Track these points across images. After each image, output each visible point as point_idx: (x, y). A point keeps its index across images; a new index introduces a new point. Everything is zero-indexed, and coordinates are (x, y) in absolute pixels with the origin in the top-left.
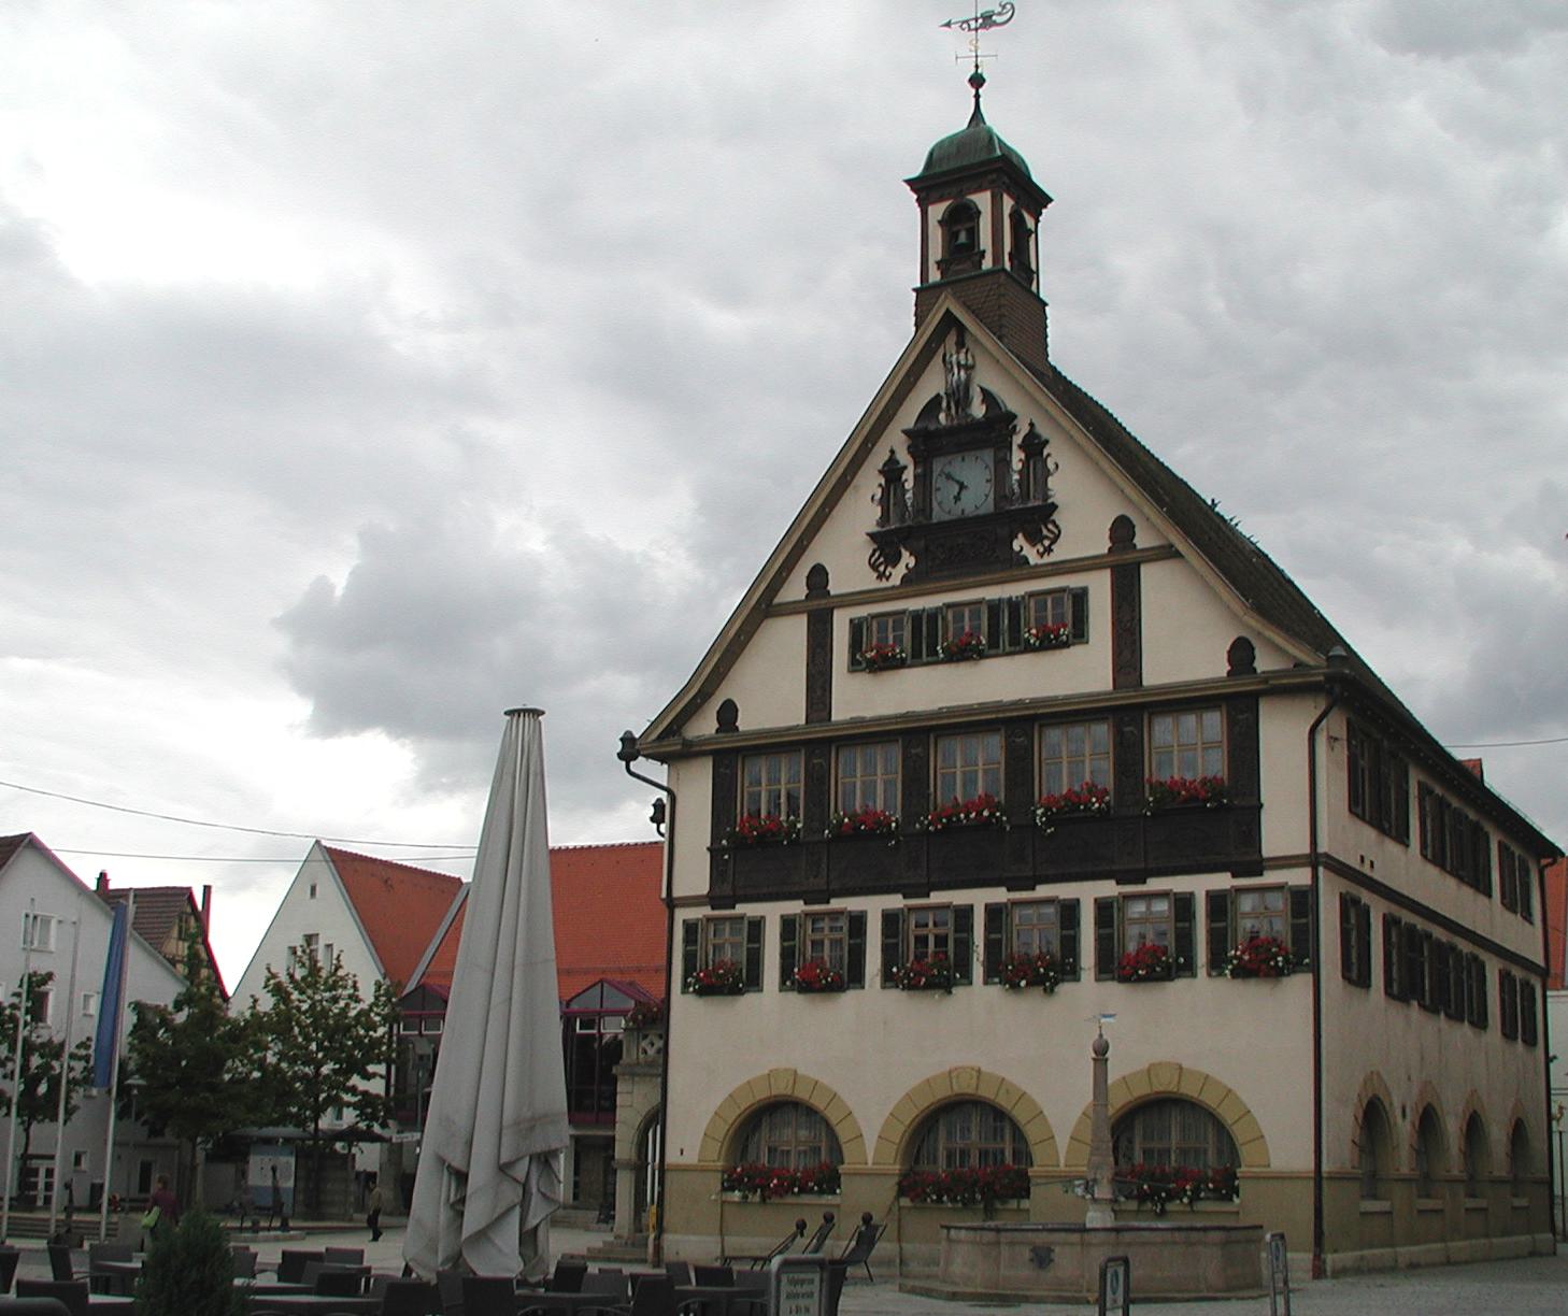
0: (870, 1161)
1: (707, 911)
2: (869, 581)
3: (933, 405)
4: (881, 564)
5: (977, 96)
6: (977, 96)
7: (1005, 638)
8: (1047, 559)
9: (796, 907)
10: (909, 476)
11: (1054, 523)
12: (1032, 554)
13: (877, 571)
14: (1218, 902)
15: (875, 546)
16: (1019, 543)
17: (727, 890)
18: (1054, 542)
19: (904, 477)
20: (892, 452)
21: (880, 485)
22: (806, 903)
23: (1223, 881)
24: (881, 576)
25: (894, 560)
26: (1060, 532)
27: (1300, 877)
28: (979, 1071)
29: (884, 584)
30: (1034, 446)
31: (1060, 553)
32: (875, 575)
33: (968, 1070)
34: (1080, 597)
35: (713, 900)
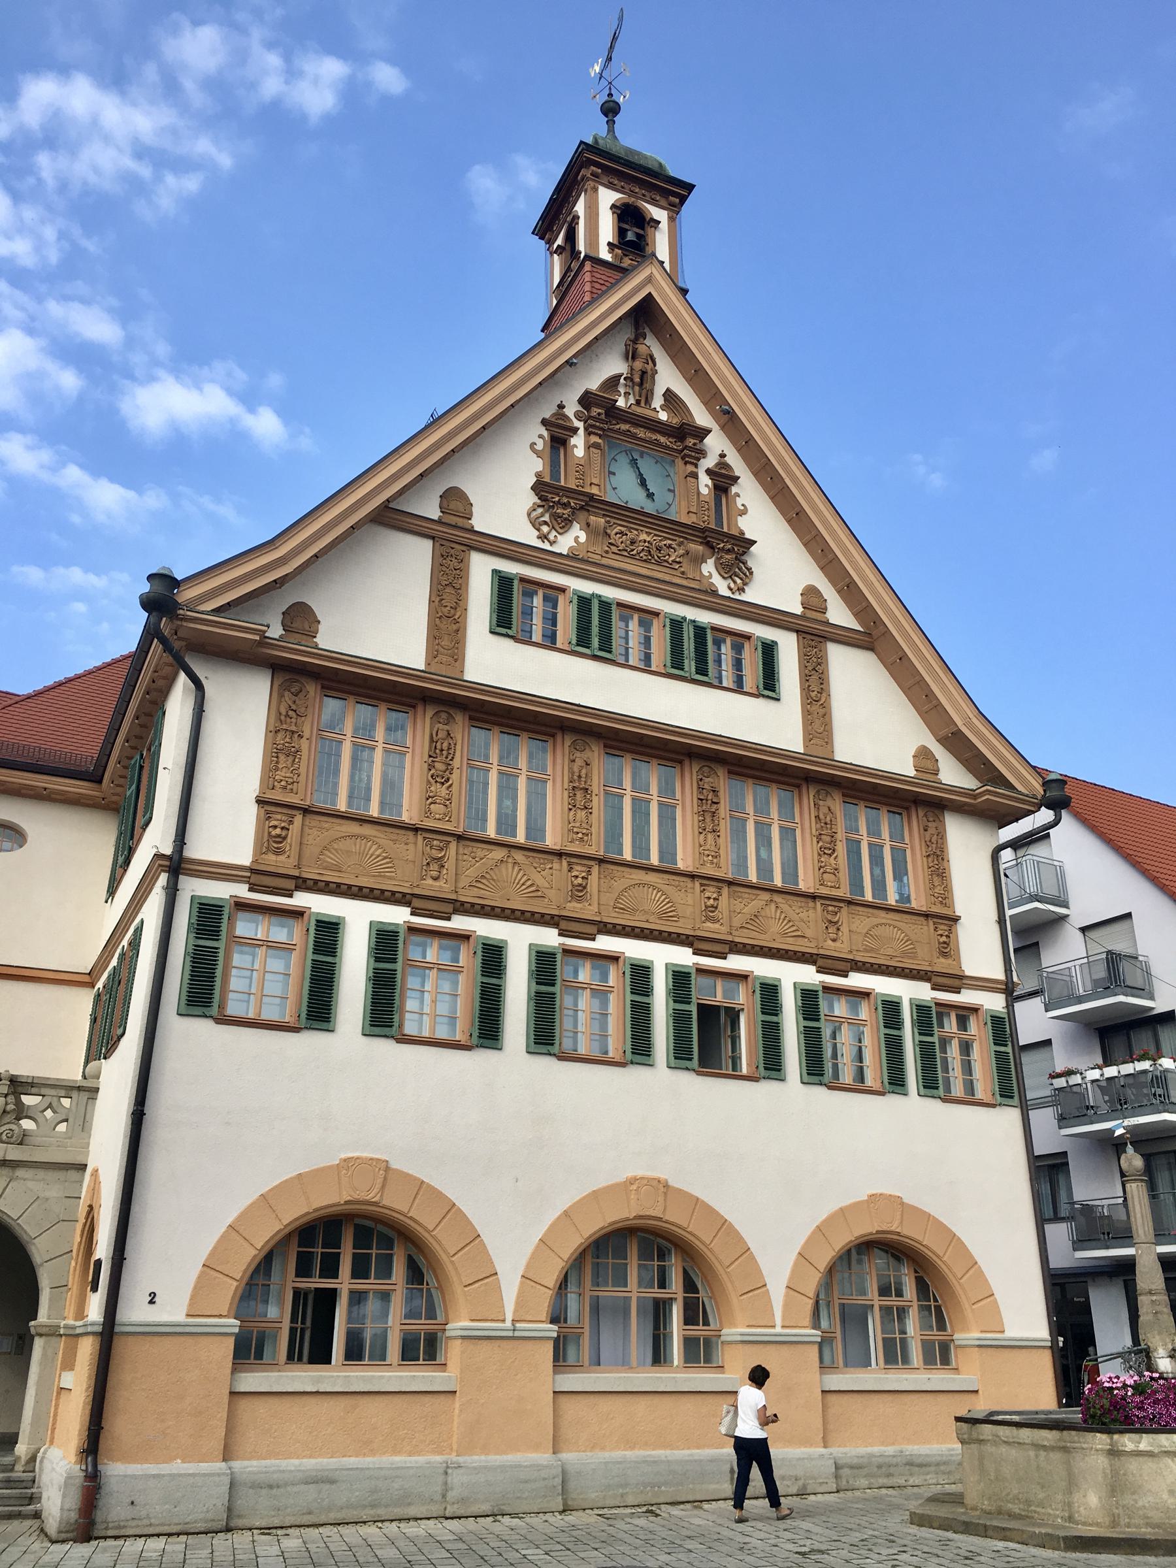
0: (509, 1317)
1: (242, 891)
2: (528, 536)
3: (612, 383)
4: (545, 523)
5: (611, 123)
6: (611, 123)
7: (690, 665)
8: (737, 596)
9: (398, 915)
10: (578, 443)
11: (744, 563)
12: (722, 587)
13: (538, 530)
14: (923, 1012)
15: (536, 500)
16: (709, 567)
17: (283, 863)
18: (745, 584)
19: (574, 441)
20: (561, 406)
21: (541, 436)
22: (412, 914)
23: (923, 992)
24: (543, 537)
25: (564, 524)
26: (751, 573)
27: (995, 1003)
28: (666, 1186)
29: (546, 546)
30: (723, 480)
31: (751, 595)
32: (537, 533)
33: (655, 1183)
34: (769, 651)
35: (256, 876)
